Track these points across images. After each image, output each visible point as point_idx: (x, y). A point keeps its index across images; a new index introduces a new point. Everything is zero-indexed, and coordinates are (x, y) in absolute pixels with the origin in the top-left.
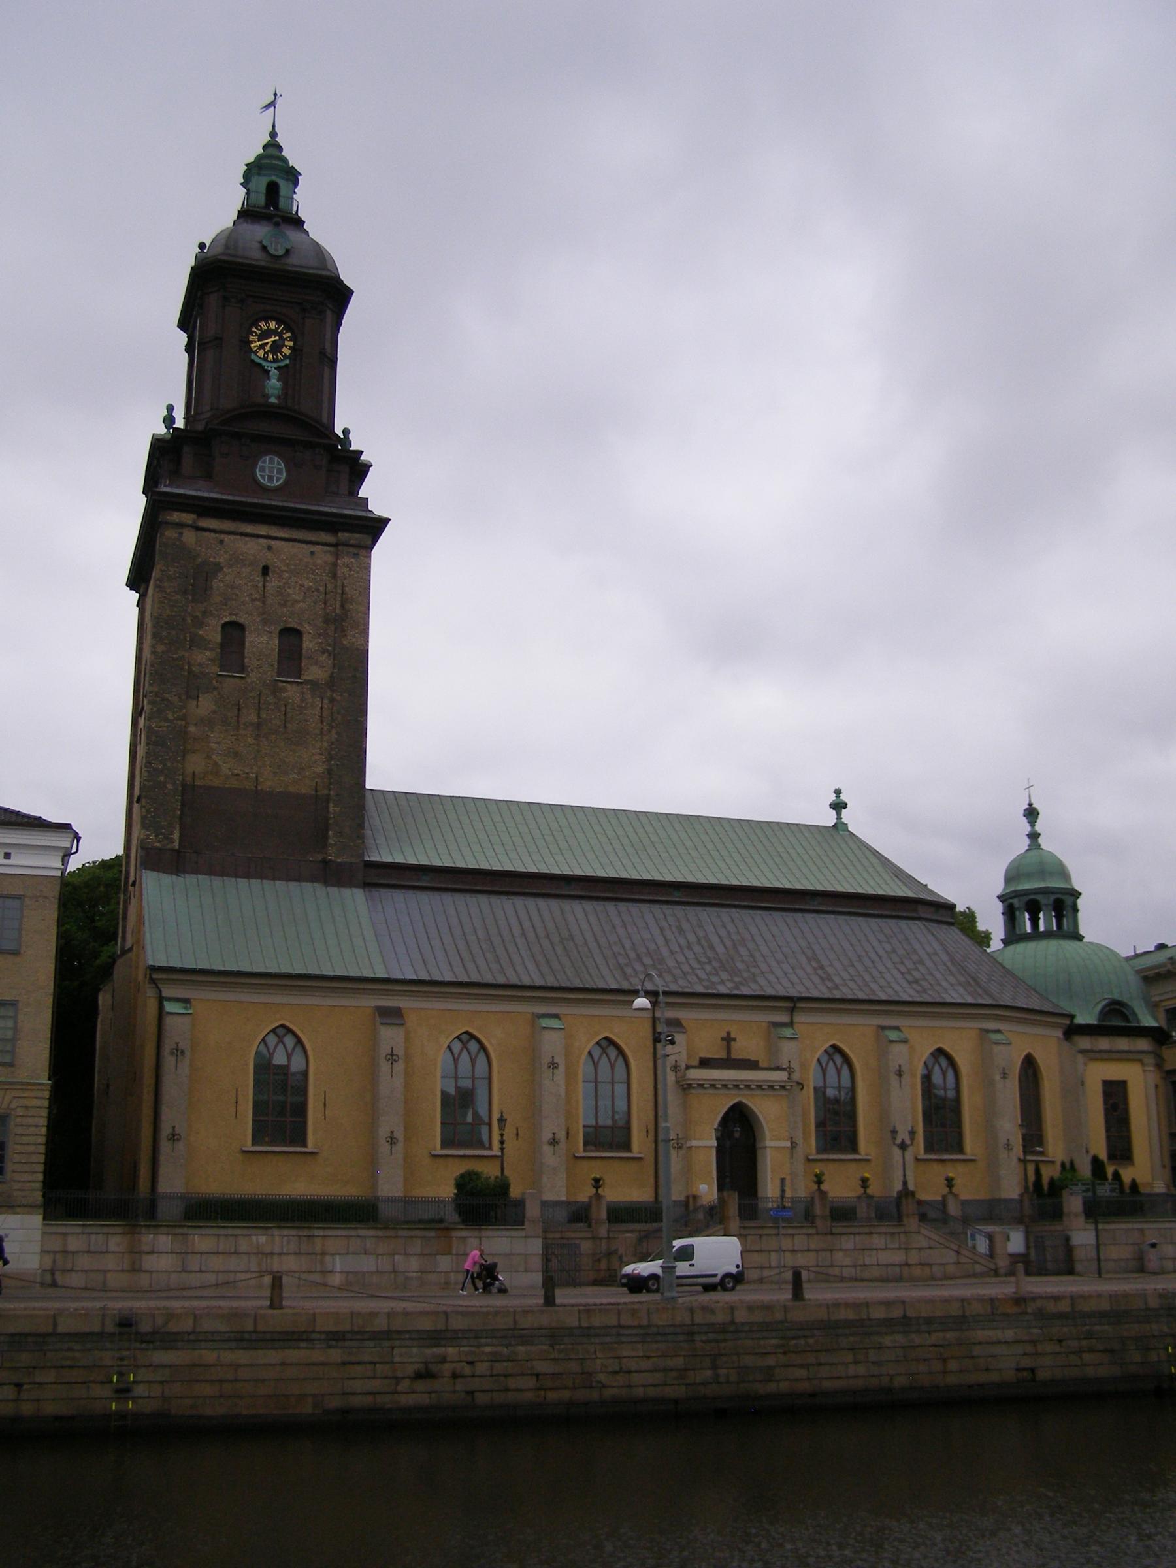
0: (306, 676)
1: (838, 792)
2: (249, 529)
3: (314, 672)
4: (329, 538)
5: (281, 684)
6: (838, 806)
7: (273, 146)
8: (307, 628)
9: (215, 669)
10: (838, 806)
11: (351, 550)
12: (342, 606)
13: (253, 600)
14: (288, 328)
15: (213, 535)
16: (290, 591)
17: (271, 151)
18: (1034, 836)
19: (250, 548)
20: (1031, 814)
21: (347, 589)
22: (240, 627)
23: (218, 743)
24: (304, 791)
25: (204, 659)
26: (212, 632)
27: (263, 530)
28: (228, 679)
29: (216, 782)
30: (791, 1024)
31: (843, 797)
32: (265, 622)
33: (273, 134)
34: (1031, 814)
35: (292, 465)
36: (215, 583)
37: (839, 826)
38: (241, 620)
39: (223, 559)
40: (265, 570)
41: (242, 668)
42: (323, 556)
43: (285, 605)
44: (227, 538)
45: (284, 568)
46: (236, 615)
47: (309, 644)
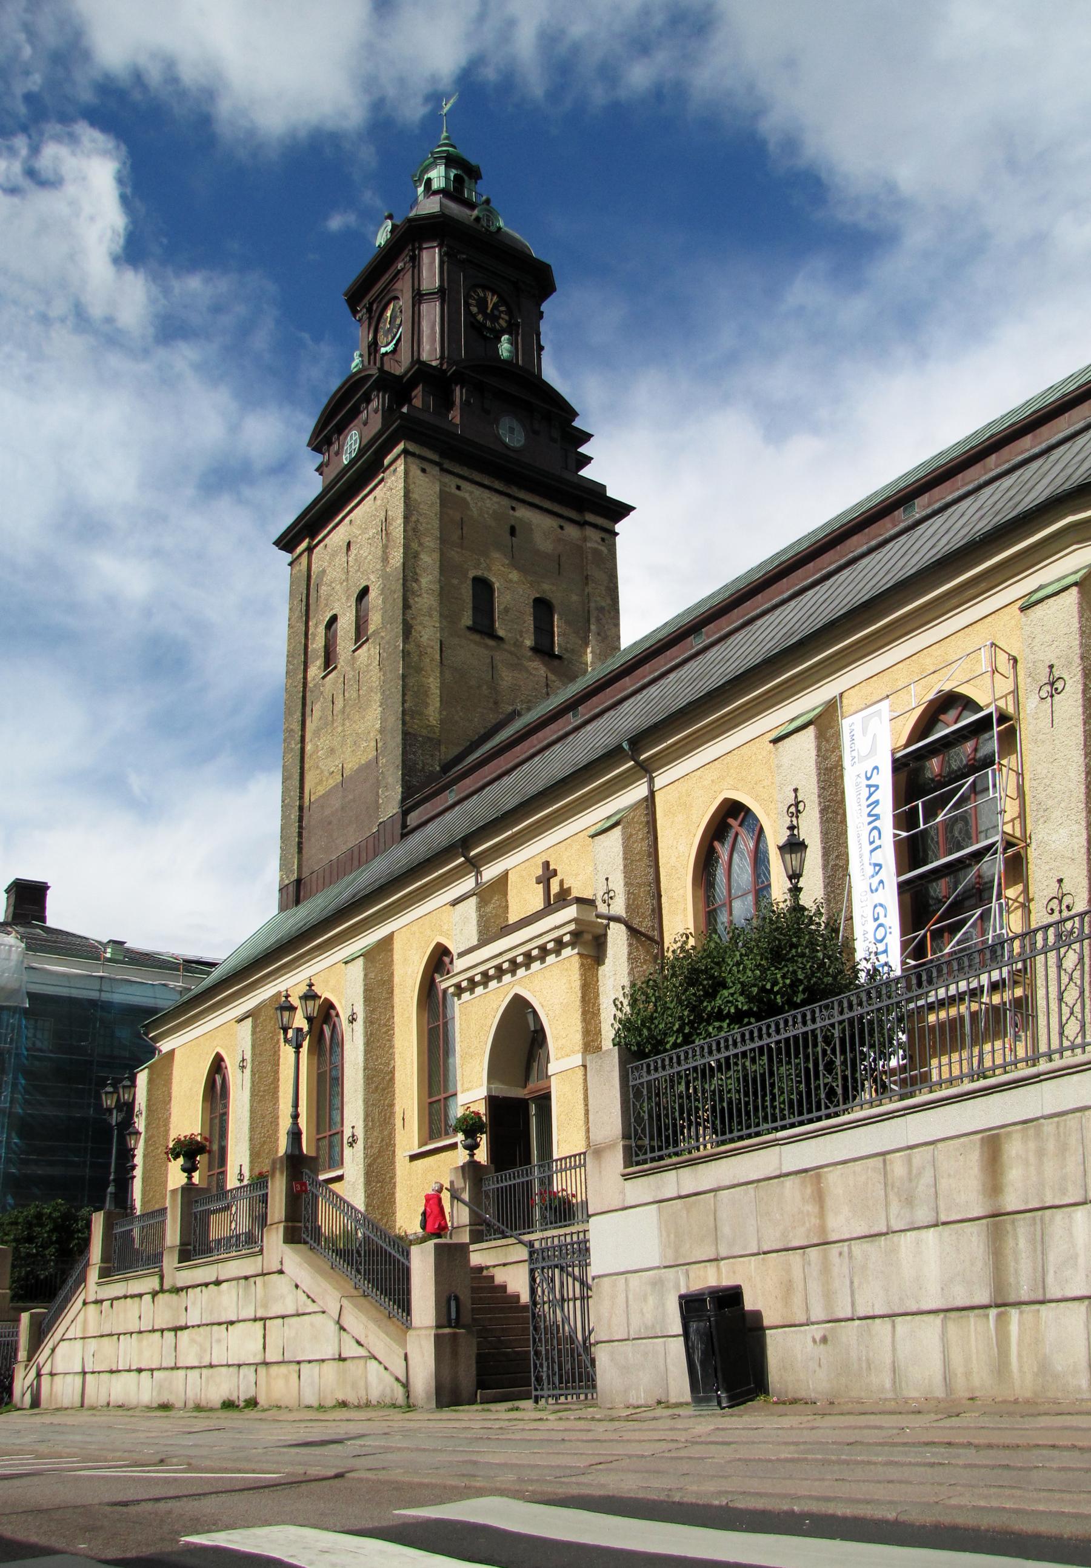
0: (372, 628)
3: (375, 620)
5: (356, 653)
11: (392, 468)
12: (387, 534)
13: (342, 583)
15: (322, 545)
16: (361, 552)
21: (389, 513)
22: (334, 619)
23: (323, 749)
24: (370, 757)
25: (315, 670)
28: (330, 676)
29: (321, 790)
32: (348, 599)
36: (324, 590)
40: (349, 544)
43: (359, 570)
44: (327, 540)
45: (358, 533)
46: (332, 609)
47: (373, 594)
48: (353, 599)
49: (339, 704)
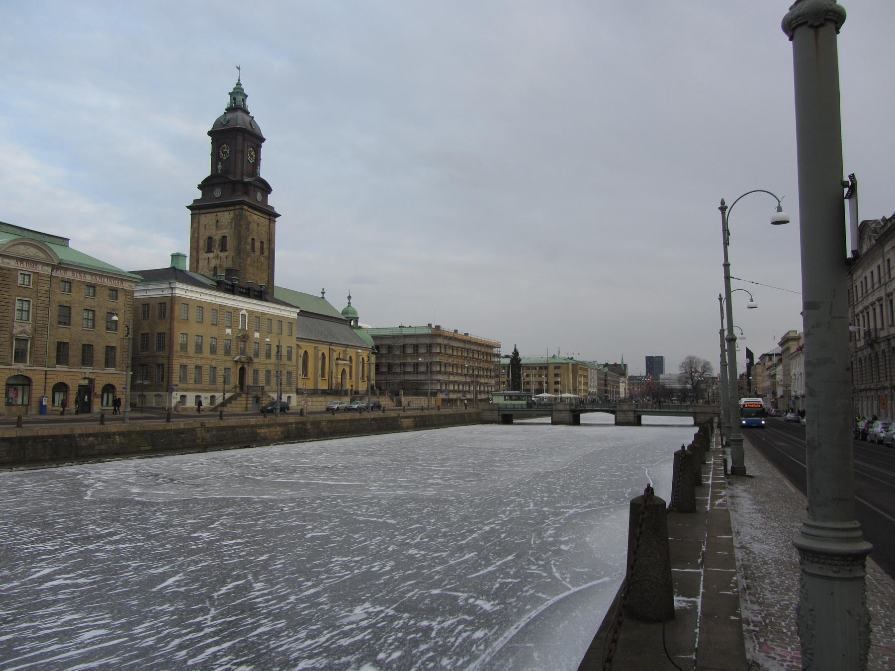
1: (323, 289)
2: (256, 212)
4: (268, 218)
6: (323, 293)
7: (239, 84)
8: (264, 242)
9: (250, 251)
10: (323, 293)
14: (254, 151)
17: (239, 86)
18: (349, 303)
19: (256, 217)
20: (349, 298)
26: (250, 241)
27: (257, 213)
30: (346, 350)
31: (324, 291)
33: (239, 80)
34: (349, 298)
35: (263, 195)
37: (323, 298)
38: (254, 238)
39: (251, 220)
41: (254, 251)
42: (267, 222)
48: (260, 241)
49: (256, 264)
